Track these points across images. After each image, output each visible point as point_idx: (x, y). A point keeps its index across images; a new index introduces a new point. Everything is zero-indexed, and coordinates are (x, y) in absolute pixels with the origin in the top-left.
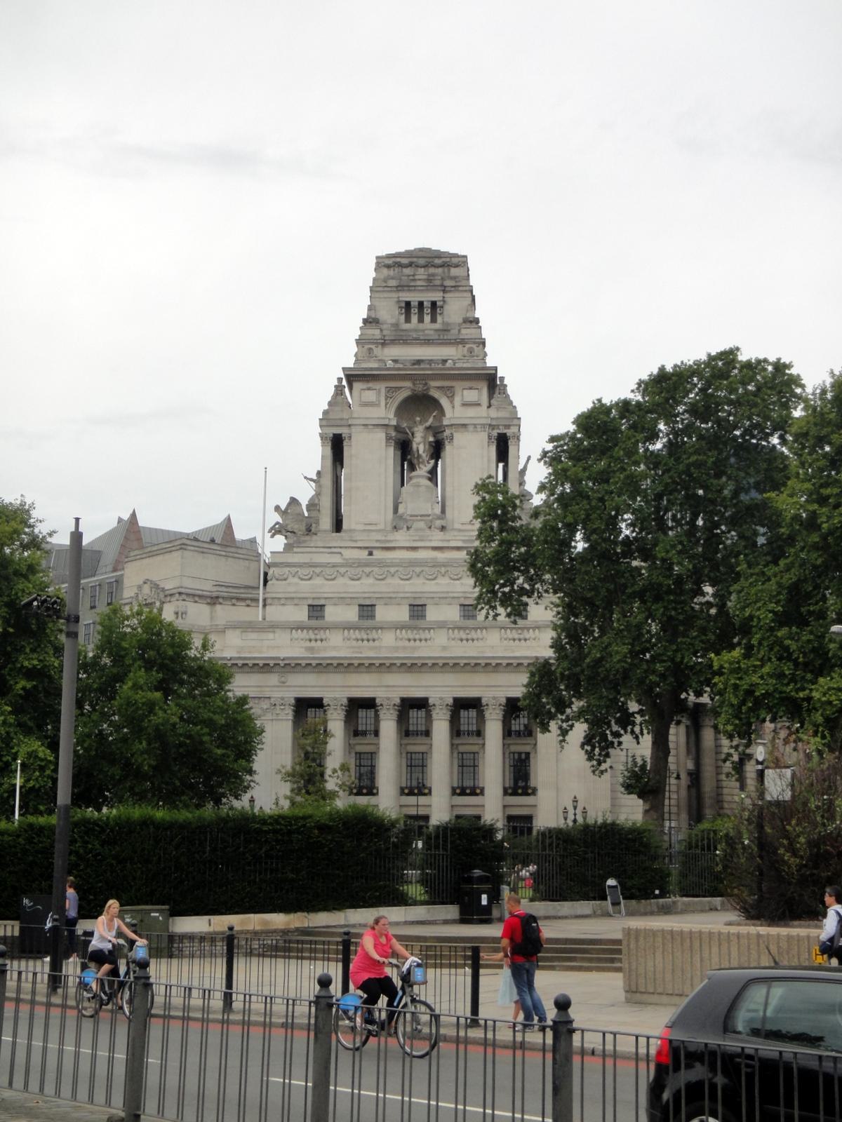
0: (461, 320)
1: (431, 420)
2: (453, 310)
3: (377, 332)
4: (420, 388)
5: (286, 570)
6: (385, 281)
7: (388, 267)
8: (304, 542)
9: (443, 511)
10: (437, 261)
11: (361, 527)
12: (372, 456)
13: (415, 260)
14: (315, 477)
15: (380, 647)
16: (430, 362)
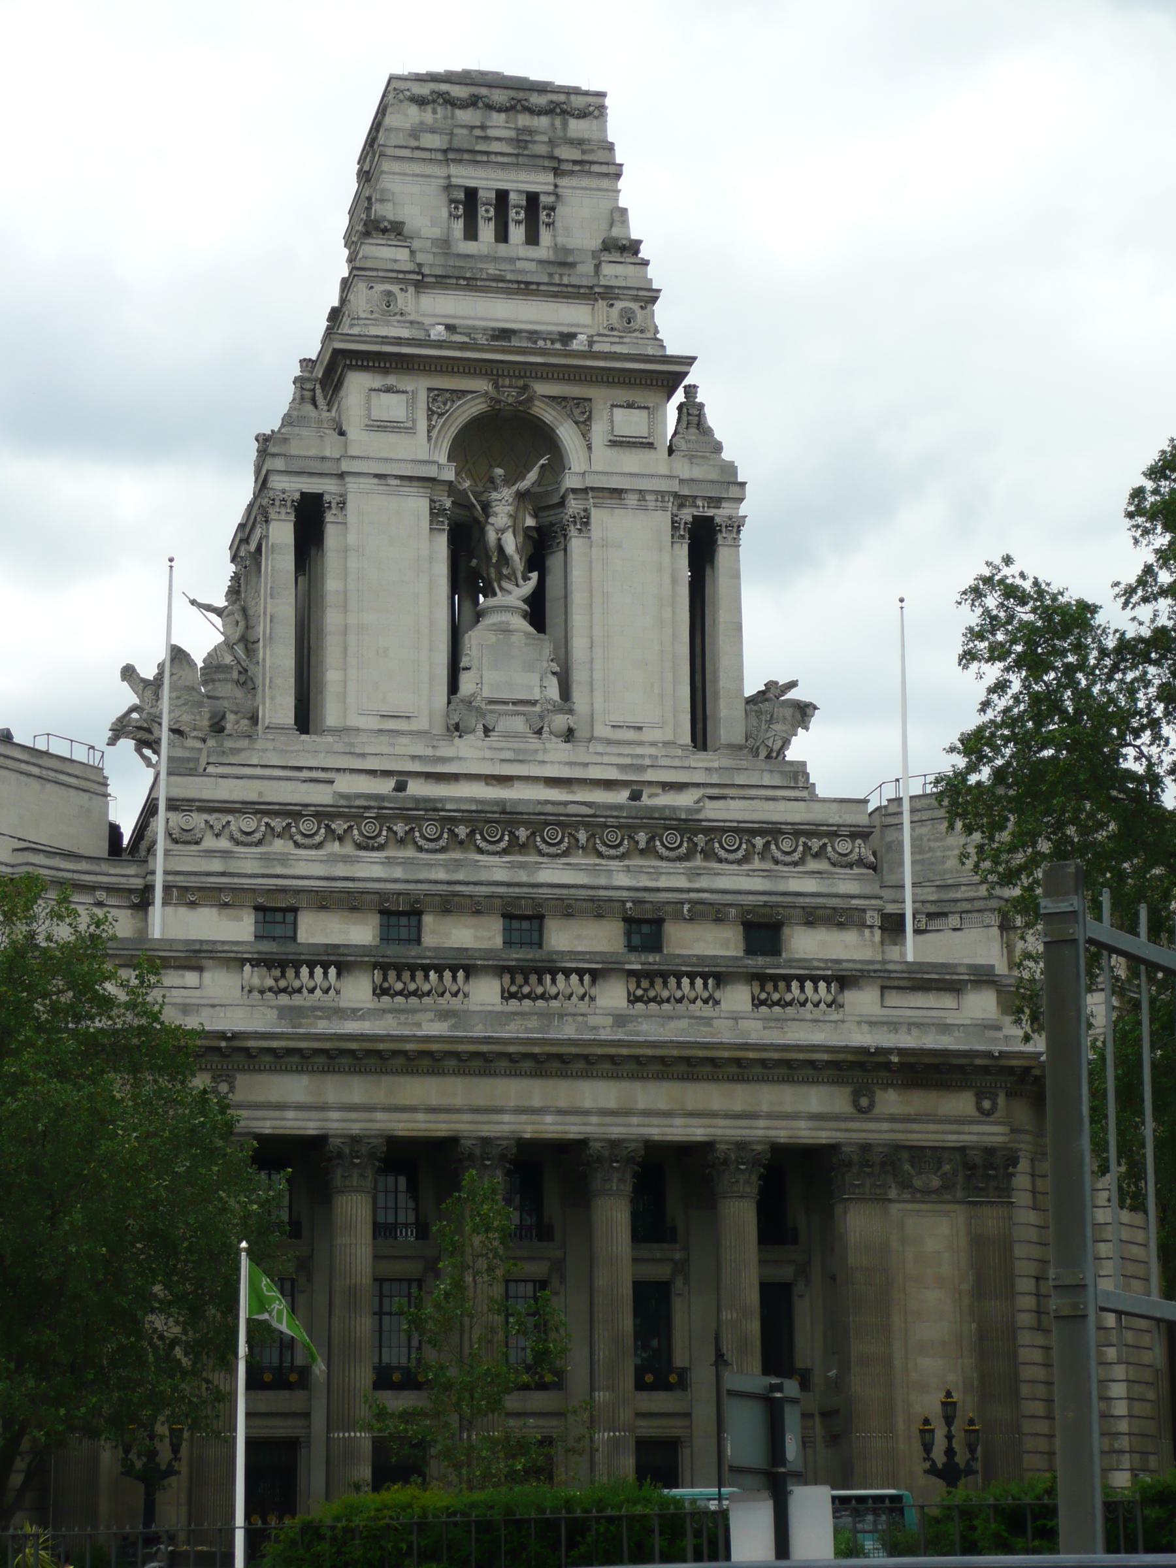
0: (595, 243)
1: (532, 476)
3: (403, 254)
5: (197, 820)
6: (415, 133)
7: (421, 102)
8: (235, 751)
10: (537, 100)
11: (374, 723)
12: (391, 556)
13: (483, 91)
14: (221, 602)
16: (533, 335)
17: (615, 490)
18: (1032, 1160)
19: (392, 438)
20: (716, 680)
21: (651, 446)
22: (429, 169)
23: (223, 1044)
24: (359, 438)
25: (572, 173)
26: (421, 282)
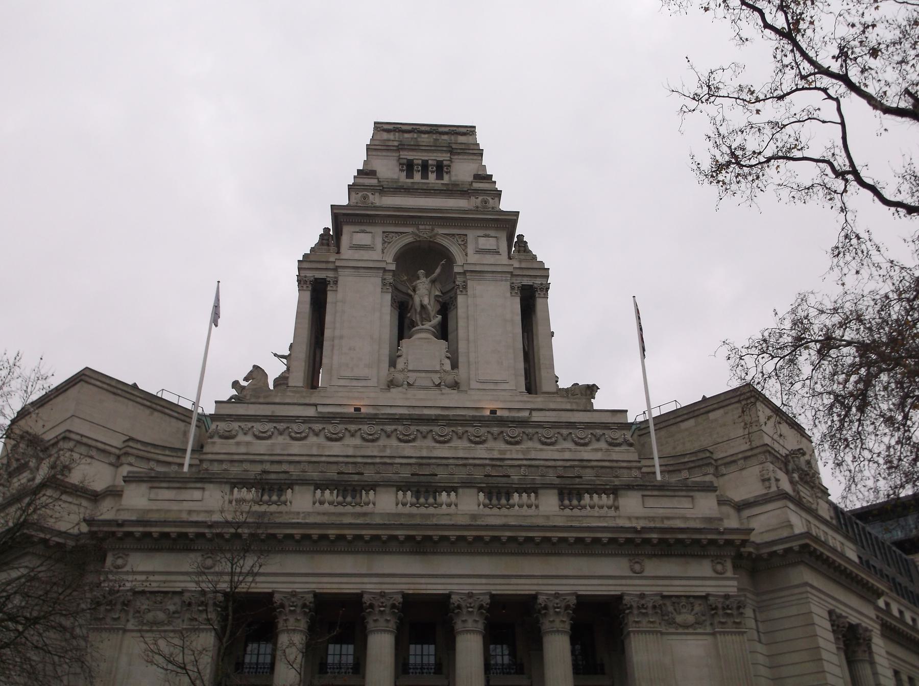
0: (471, 179)
1: (438, 271)
2: (462, 171)
3: (374, 182)
4: (424, 232)
5: (235, 425)
7: (388, 131)
9: (455, 366)
10: (441, 129)
15: (372, 514)
18: (754, 610)
19: (362, 252)
20: (539, 359)
21: (498, 253)
22: (389, 154)
23: (206, 531)
24: (346, 253)
25: (459, 154)
26: (383, 190)
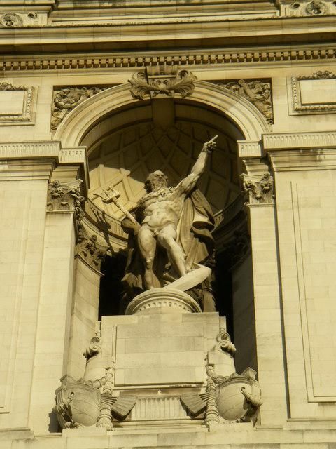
1: (200, 164)
17: (306, 150)
